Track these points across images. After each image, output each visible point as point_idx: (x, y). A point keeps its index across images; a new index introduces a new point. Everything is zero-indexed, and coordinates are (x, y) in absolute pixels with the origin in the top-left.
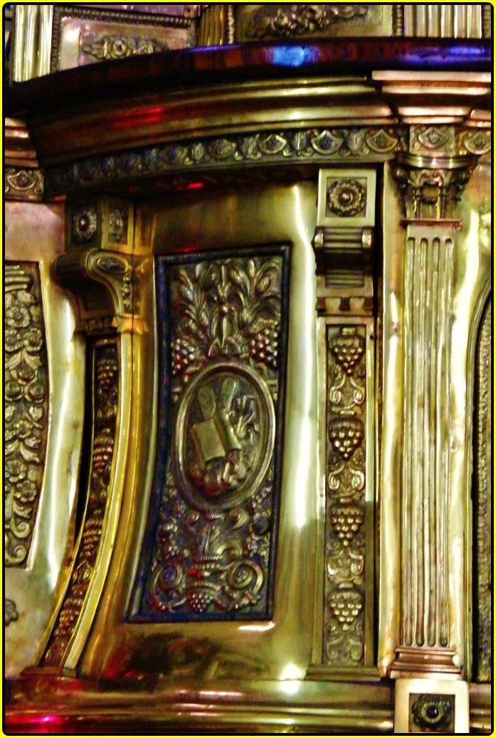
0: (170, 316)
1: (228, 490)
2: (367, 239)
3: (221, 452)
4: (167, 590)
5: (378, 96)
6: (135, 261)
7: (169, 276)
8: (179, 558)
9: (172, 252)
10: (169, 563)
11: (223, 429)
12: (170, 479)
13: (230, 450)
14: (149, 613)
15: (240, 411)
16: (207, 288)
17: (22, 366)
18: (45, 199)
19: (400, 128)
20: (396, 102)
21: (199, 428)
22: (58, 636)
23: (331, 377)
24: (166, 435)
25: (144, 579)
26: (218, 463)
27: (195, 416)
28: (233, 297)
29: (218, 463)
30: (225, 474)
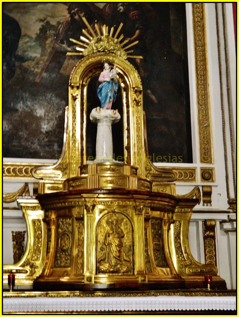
0: (58, 227)
1: (65, 250)
2: (82, 216)
3: (64, 245)
4: (58, 264)
5: (82, 197)
6: (53, 219)
7: (58, 220)
8: (59, 259)
9: (58, 217)
10: (57, 260)
11: (65, 242)
12: (58, 248)
13: (65, 244)
14: (55, 267)
15: (67, 239)
16: (62, 222)
17: (39, 233)
18: (42, 209)
19: (86, 201)
20: (85, 198)
21: (63, 242)
22: (44, 270)
23: (78, 234)
24: (58, 242)
25: (54, 262)
26: (64, 246)
27: (61, 240)
28: (66, 224)
29: (64, 246)
30: (64, 248)
